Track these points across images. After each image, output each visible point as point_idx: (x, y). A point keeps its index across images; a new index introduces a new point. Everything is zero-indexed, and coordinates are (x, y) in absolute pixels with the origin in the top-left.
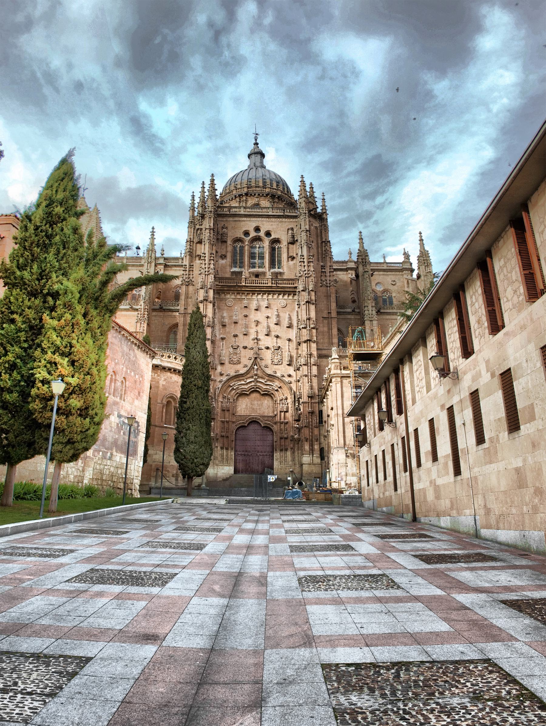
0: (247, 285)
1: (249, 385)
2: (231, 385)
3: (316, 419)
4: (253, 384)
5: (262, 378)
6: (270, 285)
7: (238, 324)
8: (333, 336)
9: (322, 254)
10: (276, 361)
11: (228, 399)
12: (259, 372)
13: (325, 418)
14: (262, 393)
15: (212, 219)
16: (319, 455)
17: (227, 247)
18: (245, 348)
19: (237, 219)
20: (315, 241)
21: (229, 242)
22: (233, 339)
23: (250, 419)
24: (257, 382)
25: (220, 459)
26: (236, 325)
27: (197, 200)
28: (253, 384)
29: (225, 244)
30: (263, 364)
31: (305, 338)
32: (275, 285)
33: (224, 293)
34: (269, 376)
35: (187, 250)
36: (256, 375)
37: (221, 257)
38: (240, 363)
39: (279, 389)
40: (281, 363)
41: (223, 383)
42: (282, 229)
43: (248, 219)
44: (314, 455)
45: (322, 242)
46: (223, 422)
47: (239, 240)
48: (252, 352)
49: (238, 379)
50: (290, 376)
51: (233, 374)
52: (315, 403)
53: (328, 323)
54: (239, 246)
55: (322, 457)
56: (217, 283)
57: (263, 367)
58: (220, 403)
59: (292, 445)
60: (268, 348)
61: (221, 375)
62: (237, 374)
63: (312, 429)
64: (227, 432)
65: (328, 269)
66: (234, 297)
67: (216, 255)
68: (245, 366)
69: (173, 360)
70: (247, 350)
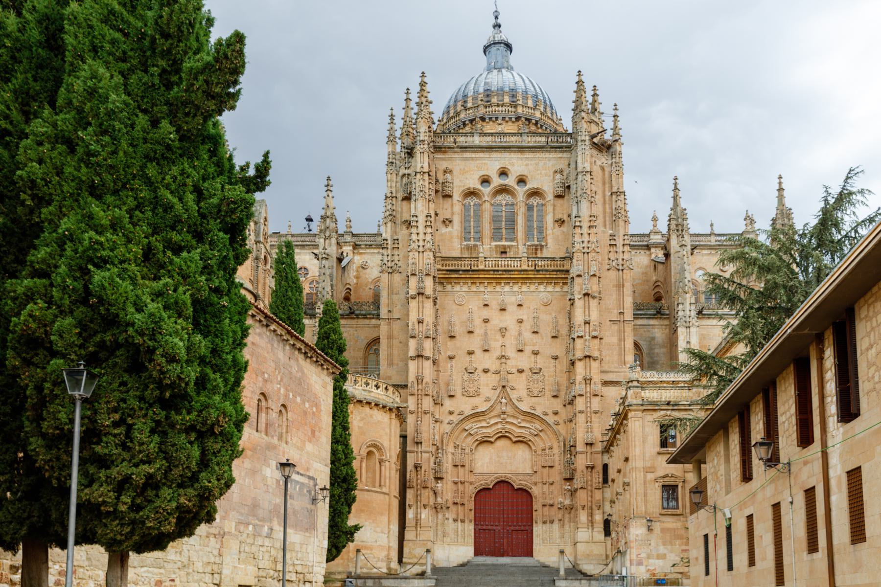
0: (487, 268)
1: (494, 428)
2: (467, 428)
3: (598, 477)
4: (500, 426)
5: (514, 417)
6: (525, 267)
7: (475, 334)
8: (627, 350)
9: (612, 215)
10: (536, 392)
11: (462, 449)
12: (509, 409)
13: (612, 474)
14: (514, 439)
15: (426, 155)
16: (602, 530)
17: (452, 205)
18: (486, 371)
19: (468, 155)
20: (600, 192)
21: (457, 196)
22: (468, 358)
23: (496, 478)
24: (507, 422)
25: (452, 535)
26: (472, 335)
27: (399, 123)
28: (500, 426)
29: (449, 200)
30: (514, 395)
31: (579, 354)
32: (533, 268)
33: (451, 283)
34: (525, 413)
35: (388, 213)
36: (504, 413)
37: (444, 222)
38: (479, 395)
39: (540, 434)
40: (541, 394)
41: (454, 425)
42: (544, 172)
43: (487, 155)
44: (595, 530)
45: (612, 194)
46: (456, 483)
47: (471, 193)
48: (497, 377)
49: (476, 419)
50: (556, 413)
51: (468, 412)
52: (597, 453)
53: (619, 331)
54: (472, 204)
55: (607, 532)
56: (439, 267)
57: (515, 401)
58: (450, 456)
59: (560, 516)
60: (521, 371)
61: (451, 413)
62: (475, 411)
63: (591, 491)
64: (462, 497)
65: (621, 238)
66: (467, 290)
67: (435, 220)
68: (488, 400)
69: (374, 389)
70: (489, 374)
